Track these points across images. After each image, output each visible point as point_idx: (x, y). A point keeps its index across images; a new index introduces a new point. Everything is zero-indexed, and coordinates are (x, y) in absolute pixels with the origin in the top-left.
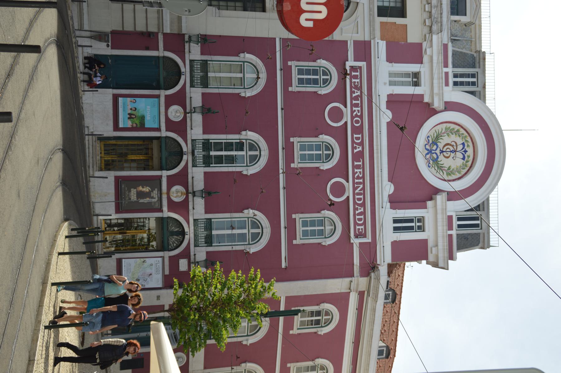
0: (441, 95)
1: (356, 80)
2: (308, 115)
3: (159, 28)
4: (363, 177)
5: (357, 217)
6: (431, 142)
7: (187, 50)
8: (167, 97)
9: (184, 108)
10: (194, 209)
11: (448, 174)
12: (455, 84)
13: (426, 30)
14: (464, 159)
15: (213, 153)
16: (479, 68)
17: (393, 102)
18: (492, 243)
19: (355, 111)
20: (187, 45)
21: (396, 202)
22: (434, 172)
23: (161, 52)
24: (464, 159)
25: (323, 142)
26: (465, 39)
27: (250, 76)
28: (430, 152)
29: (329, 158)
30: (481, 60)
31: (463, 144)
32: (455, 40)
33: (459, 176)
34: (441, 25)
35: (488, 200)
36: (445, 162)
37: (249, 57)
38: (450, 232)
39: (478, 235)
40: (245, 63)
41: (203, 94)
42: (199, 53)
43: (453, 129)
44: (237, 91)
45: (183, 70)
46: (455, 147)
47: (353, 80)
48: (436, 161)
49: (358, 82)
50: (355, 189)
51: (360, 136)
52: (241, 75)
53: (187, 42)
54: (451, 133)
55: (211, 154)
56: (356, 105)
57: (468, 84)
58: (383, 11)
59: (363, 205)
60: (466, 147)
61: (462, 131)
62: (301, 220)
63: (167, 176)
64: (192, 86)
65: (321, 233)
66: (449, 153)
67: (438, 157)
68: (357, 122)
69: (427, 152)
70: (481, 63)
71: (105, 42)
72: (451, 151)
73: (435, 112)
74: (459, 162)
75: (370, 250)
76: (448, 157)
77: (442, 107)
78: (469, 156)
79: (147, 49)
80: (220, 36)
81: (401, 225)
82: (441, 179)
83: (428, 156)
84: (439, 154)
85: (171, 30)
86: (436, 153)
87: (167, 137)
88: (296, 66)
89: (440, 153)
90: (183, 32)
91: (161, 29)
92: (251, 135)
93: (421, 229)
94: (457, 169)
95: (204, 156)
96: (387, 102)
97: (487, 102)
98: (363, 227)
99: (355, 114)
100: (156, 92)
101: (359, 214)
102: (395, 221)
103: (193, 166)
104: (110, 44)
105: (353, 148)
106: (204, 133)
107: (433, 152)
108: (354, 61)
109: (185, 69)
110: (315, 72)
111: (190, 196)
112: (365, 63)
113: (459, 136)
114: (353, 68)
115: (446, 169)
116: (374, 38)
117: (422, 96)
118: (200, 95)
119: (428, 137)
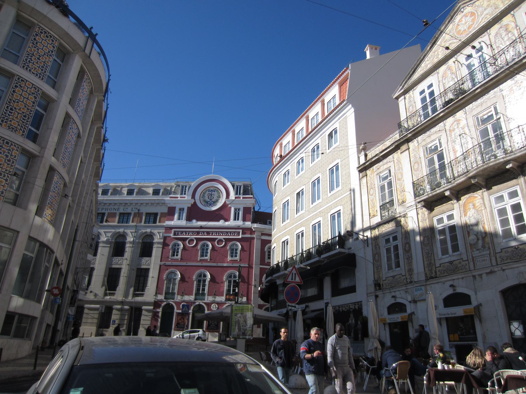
12: (185, 194)
17: (189, 219)
23: (160, 310)
28: (210, 204)
38: (241, 198)
39: (244, 186)
50: (220, 235)
58: (155, 222)
59: (227, 232)
65: (236, 250)
73: (195, 203)
74: (216, 193)
81: (236, 218)
100: (175, 314)
105: (205, 235)
114: (175, 234)
117: (188, 207)
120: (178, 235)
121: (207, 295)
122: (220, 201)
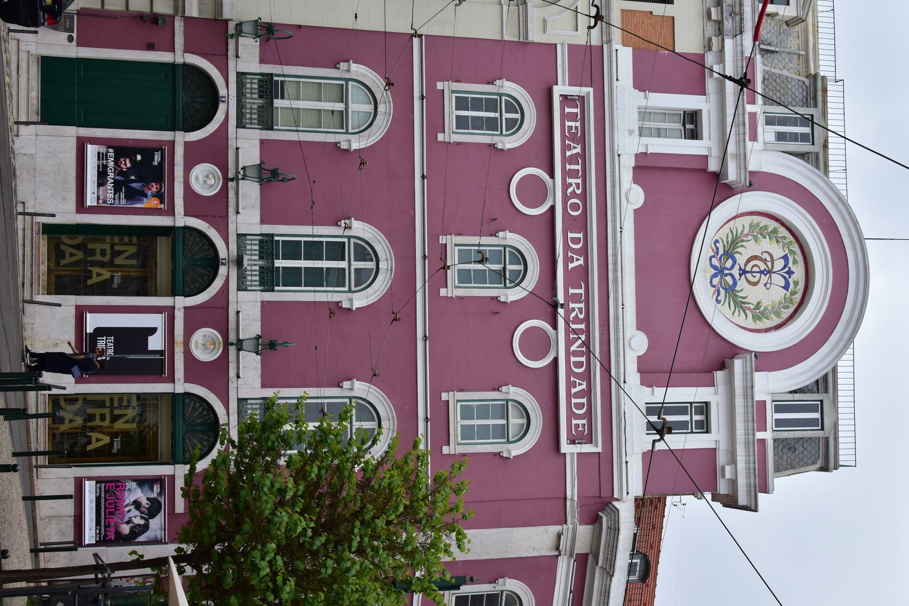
0: (742, 158)
1: (573, 124)
2: (476, 191)
3: (176, 8)
4: (587, 320)
5: (574, 401)
6: (721, 252)
7: (231, 53)
8: (187, 145)
9: (224, 169)
10: (238, 377)
11: (756, 318)
13: (710, 29)
14: (786, 287)
15: (280, 263)
16: (816, 106)
17: (647, 168)
18: (842, 460)
19: (571, 185)
20: (231, 44)
21: (651, 372)
22: (729, 314)
23: (180, 56)
24: (786, 287)
25: (505, 247)
26: (787, 50)
27: (358, 107)
28: (720, 272)
29: (518, 279)
30: (820, 93)
31: (785, 258)
32: (767, 51)
33: (778, 321)
34: (742, 19)
35: (834, 370)
36: (750, 293)
37: (358, 70)
38: (760, 435)
40: (350, 83)
41: (262, 142)
42: (257, 59)
43: (766, 227)
44: (330, 138)
45: (222, 92)
46: (769, 264)
47: (568, 124)
48: (731, 290)
49: (576, 128)
50: (569, 343)
51: (580, 235)
52: (340, 106)
53: (232, 36)
54: (762, 234)
55: (276, 265)
56: (574, 174)
57: (794, 137)
59: (587, 376)
60: (790, 265)
61: (783, 232)
62: (459, 404)
63: (185, 308)
64: (240, 125)
66: (758, 275)
67: (735, 283)
68: (575, 207)
69: (713, 271)
70: (820, 98)
71: (66, 30)
72: (761, 272)
73: (729, 191)
75: (601, 468)
76: (755, 284)
77: (744, 180)
78: (796, 283)
79: (150, 47)
80: (300, 26)
82: (742, 327)
83: (716, 281)
84: (737, 277)
85: (200, 13)
86: (732, 275)
87: (187, 229)
88: (453, 92)
89: (740, 275)
90: (226, 15)
91: (180, 10)
92: (360, 229)
93: (704, 427)
94: (773, 307)
95: (261, 268)
96: (636, 169)
97: (831, 175)
98: (584, 421)
99: (570, 190)
100: (166, 136)
101: (578, 395)
102: (651, 410)
103: (238, 290)
104: (75, 35)
105: (568, 260)
106: (263, 221)
107: (726, 272)
108: (570, 85)
109: (228, 90)
110: (492, 105)
111: (232, 350)
112: (591, 90)
113: (777, 242)
114: (566, 99)
115: (752, 307)
116: (609, 41)
117: (705, 158)
118: (258, 143)
119: (717, 241)
120: (564, 117)
121: (269, 296)
122: (741, 320)
